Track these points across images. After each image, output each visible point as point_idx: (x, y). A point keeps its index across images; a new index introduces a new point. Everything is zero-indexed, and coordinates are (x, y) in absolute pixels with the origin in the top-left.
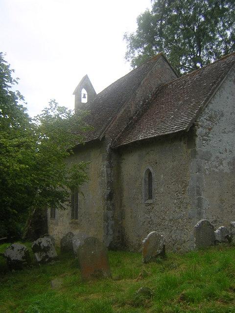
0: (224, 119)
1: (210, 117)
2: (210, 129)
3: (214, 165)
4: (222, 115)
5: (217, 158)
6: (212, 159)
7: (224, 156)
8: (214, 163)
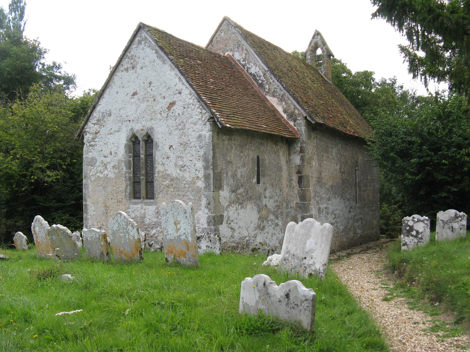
0: (112, 117)
1: (98, 120)
2: (96, 133)
3: (99, 170)
4: (110, 115)
5: (102, 162)
6: (98, 164)
7: (108, 160)
8: (99, 169)
